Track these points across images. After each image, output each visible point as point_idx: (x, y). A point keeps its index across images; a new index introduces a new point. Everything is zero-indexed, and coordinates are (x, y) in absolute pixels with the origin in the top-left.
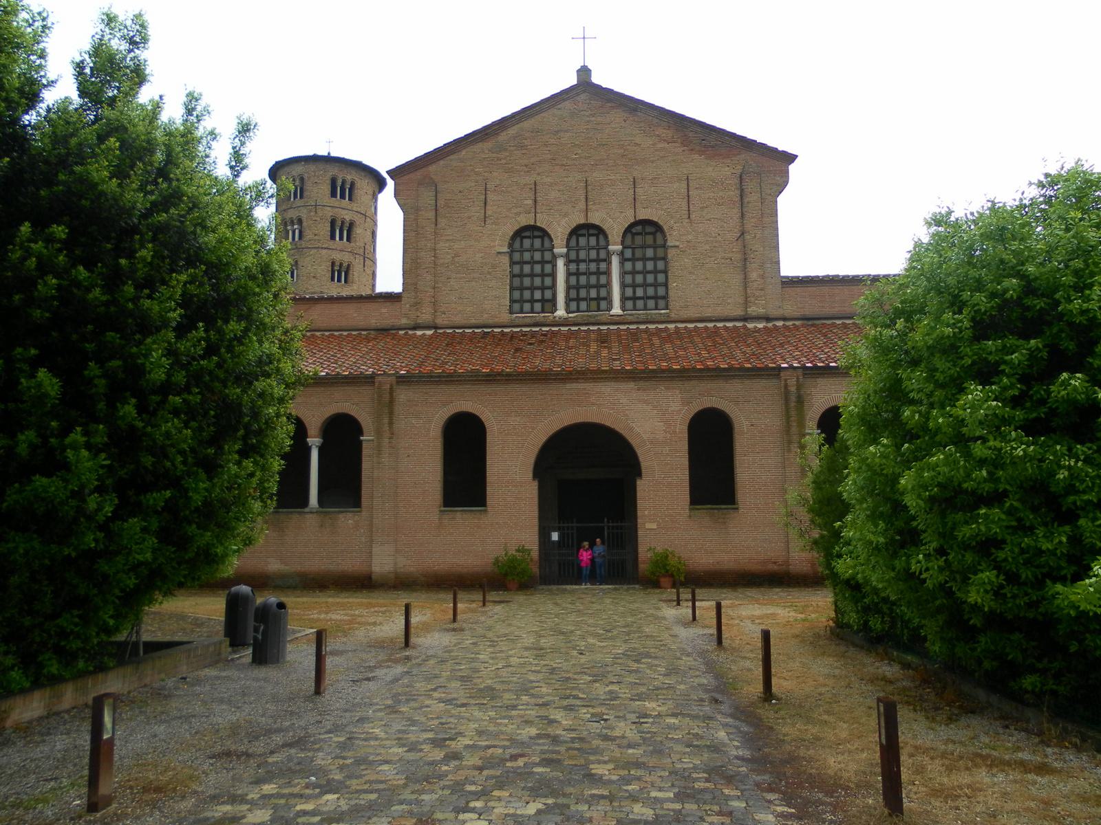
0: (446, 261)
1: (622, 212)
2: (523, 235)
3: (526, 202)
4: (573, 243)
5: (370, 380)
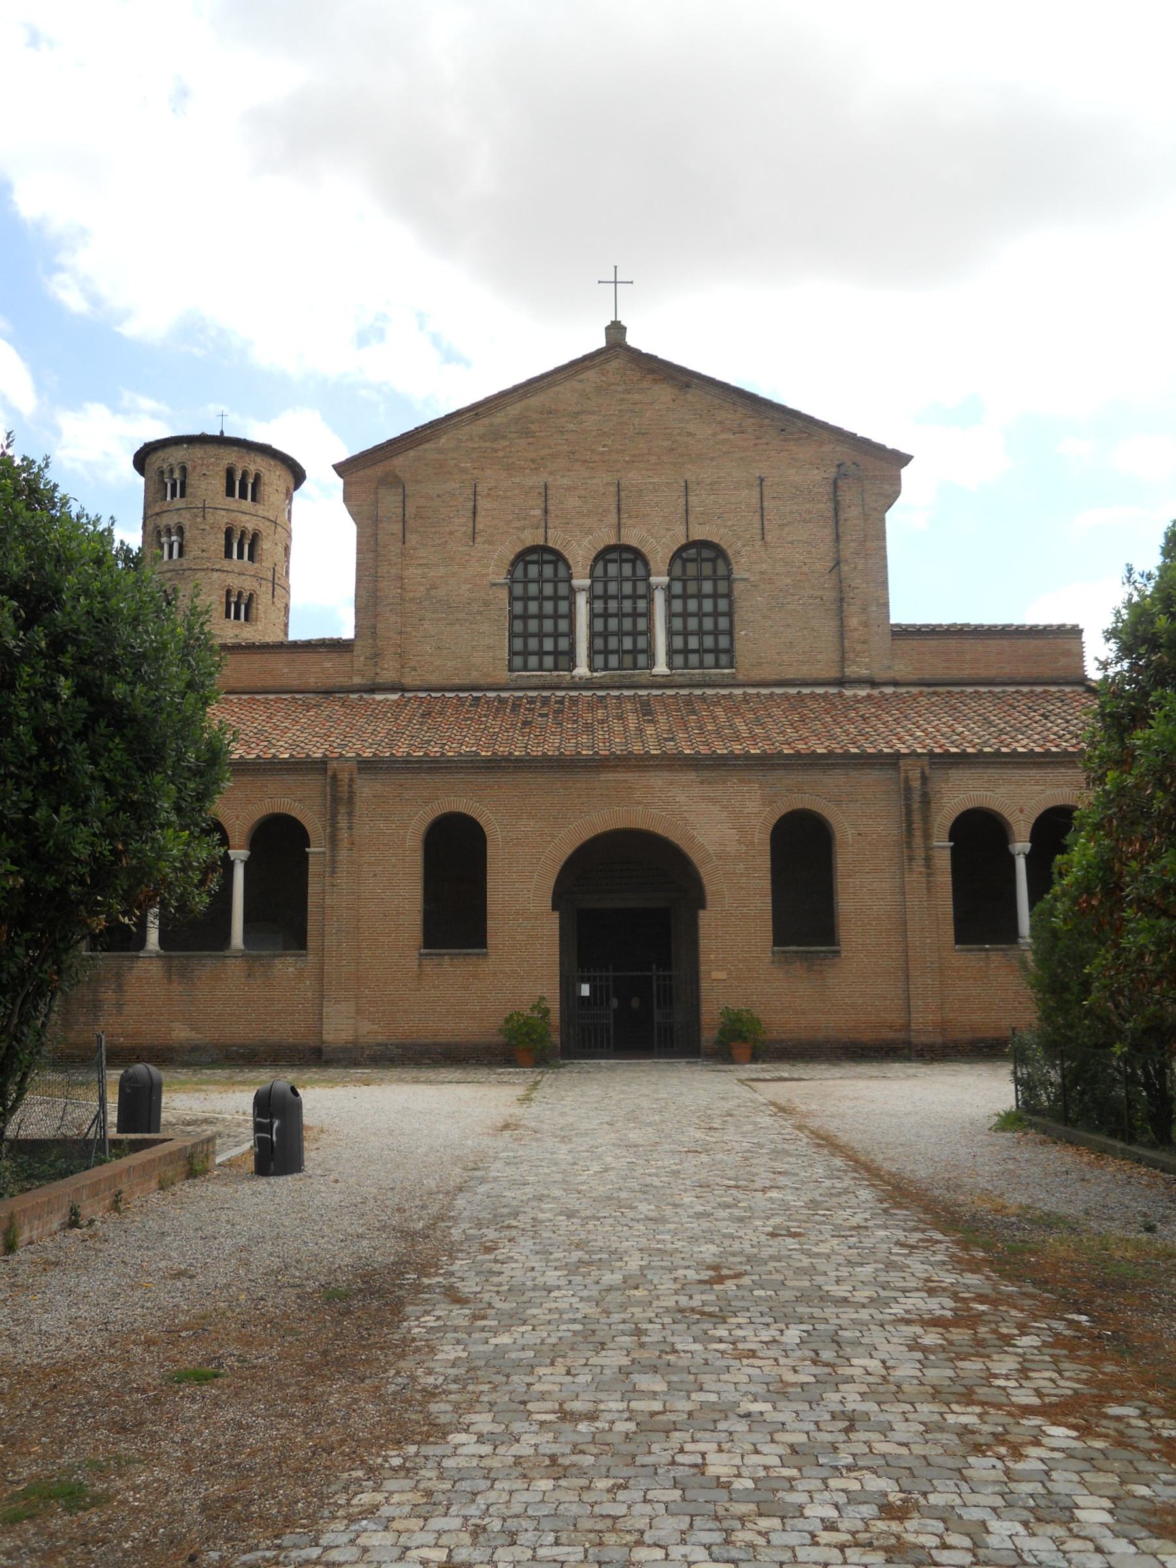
0: (418, 595)
1: (668, 530)
2: (528, 558)
3: (532, 512)
4: (599, 571)
5: (320, 766)
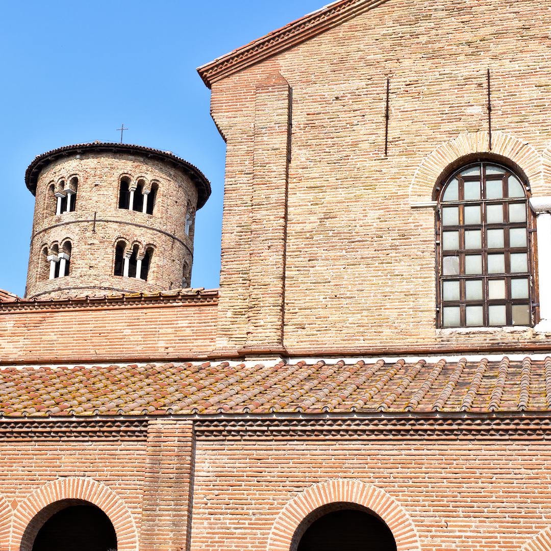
0: (308, 227)
